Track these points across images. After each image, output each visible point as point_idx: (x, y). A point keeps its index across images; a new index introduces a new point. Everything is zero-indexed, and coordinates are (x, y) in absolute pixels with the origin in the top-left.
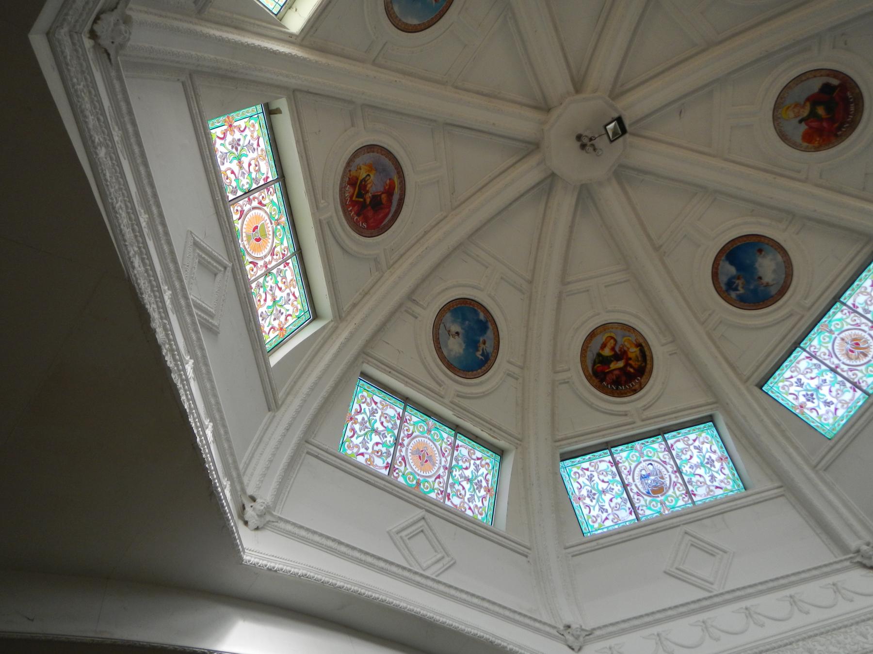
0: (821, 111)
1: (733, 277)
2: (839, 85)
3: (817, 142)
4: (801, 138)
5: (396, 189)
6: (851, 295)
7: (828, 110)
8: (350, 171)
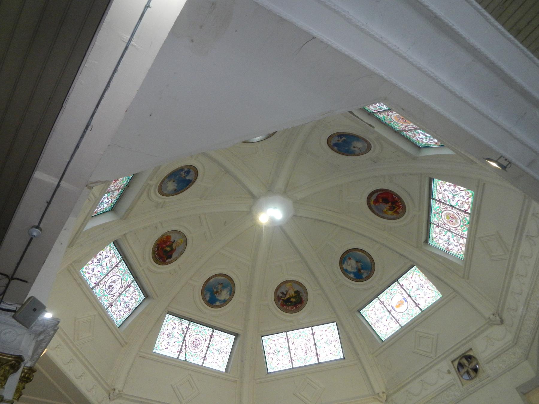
0: (168, 249)
1: (187, 176)
2: (166, 260)
3: (164, 238)
4: (171, 236)
5: (373, 200)
6: (120, 192)
7: (166, 251)
8: (397, 216)
